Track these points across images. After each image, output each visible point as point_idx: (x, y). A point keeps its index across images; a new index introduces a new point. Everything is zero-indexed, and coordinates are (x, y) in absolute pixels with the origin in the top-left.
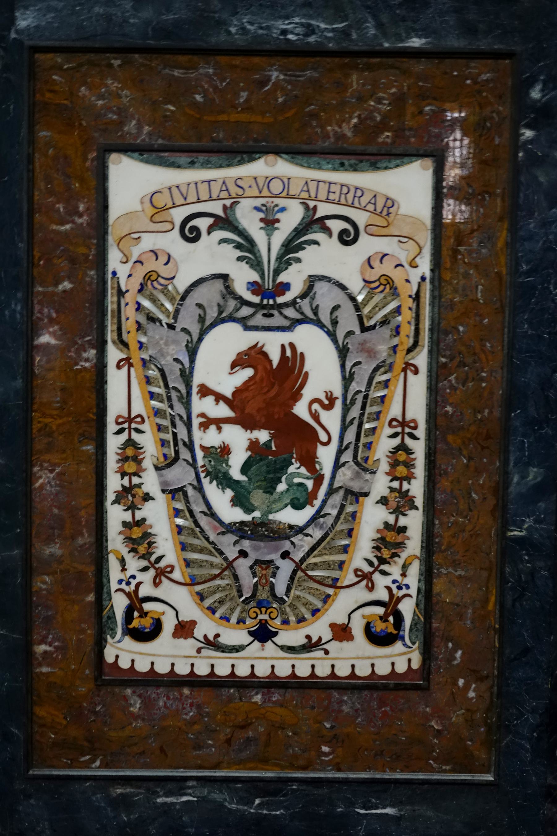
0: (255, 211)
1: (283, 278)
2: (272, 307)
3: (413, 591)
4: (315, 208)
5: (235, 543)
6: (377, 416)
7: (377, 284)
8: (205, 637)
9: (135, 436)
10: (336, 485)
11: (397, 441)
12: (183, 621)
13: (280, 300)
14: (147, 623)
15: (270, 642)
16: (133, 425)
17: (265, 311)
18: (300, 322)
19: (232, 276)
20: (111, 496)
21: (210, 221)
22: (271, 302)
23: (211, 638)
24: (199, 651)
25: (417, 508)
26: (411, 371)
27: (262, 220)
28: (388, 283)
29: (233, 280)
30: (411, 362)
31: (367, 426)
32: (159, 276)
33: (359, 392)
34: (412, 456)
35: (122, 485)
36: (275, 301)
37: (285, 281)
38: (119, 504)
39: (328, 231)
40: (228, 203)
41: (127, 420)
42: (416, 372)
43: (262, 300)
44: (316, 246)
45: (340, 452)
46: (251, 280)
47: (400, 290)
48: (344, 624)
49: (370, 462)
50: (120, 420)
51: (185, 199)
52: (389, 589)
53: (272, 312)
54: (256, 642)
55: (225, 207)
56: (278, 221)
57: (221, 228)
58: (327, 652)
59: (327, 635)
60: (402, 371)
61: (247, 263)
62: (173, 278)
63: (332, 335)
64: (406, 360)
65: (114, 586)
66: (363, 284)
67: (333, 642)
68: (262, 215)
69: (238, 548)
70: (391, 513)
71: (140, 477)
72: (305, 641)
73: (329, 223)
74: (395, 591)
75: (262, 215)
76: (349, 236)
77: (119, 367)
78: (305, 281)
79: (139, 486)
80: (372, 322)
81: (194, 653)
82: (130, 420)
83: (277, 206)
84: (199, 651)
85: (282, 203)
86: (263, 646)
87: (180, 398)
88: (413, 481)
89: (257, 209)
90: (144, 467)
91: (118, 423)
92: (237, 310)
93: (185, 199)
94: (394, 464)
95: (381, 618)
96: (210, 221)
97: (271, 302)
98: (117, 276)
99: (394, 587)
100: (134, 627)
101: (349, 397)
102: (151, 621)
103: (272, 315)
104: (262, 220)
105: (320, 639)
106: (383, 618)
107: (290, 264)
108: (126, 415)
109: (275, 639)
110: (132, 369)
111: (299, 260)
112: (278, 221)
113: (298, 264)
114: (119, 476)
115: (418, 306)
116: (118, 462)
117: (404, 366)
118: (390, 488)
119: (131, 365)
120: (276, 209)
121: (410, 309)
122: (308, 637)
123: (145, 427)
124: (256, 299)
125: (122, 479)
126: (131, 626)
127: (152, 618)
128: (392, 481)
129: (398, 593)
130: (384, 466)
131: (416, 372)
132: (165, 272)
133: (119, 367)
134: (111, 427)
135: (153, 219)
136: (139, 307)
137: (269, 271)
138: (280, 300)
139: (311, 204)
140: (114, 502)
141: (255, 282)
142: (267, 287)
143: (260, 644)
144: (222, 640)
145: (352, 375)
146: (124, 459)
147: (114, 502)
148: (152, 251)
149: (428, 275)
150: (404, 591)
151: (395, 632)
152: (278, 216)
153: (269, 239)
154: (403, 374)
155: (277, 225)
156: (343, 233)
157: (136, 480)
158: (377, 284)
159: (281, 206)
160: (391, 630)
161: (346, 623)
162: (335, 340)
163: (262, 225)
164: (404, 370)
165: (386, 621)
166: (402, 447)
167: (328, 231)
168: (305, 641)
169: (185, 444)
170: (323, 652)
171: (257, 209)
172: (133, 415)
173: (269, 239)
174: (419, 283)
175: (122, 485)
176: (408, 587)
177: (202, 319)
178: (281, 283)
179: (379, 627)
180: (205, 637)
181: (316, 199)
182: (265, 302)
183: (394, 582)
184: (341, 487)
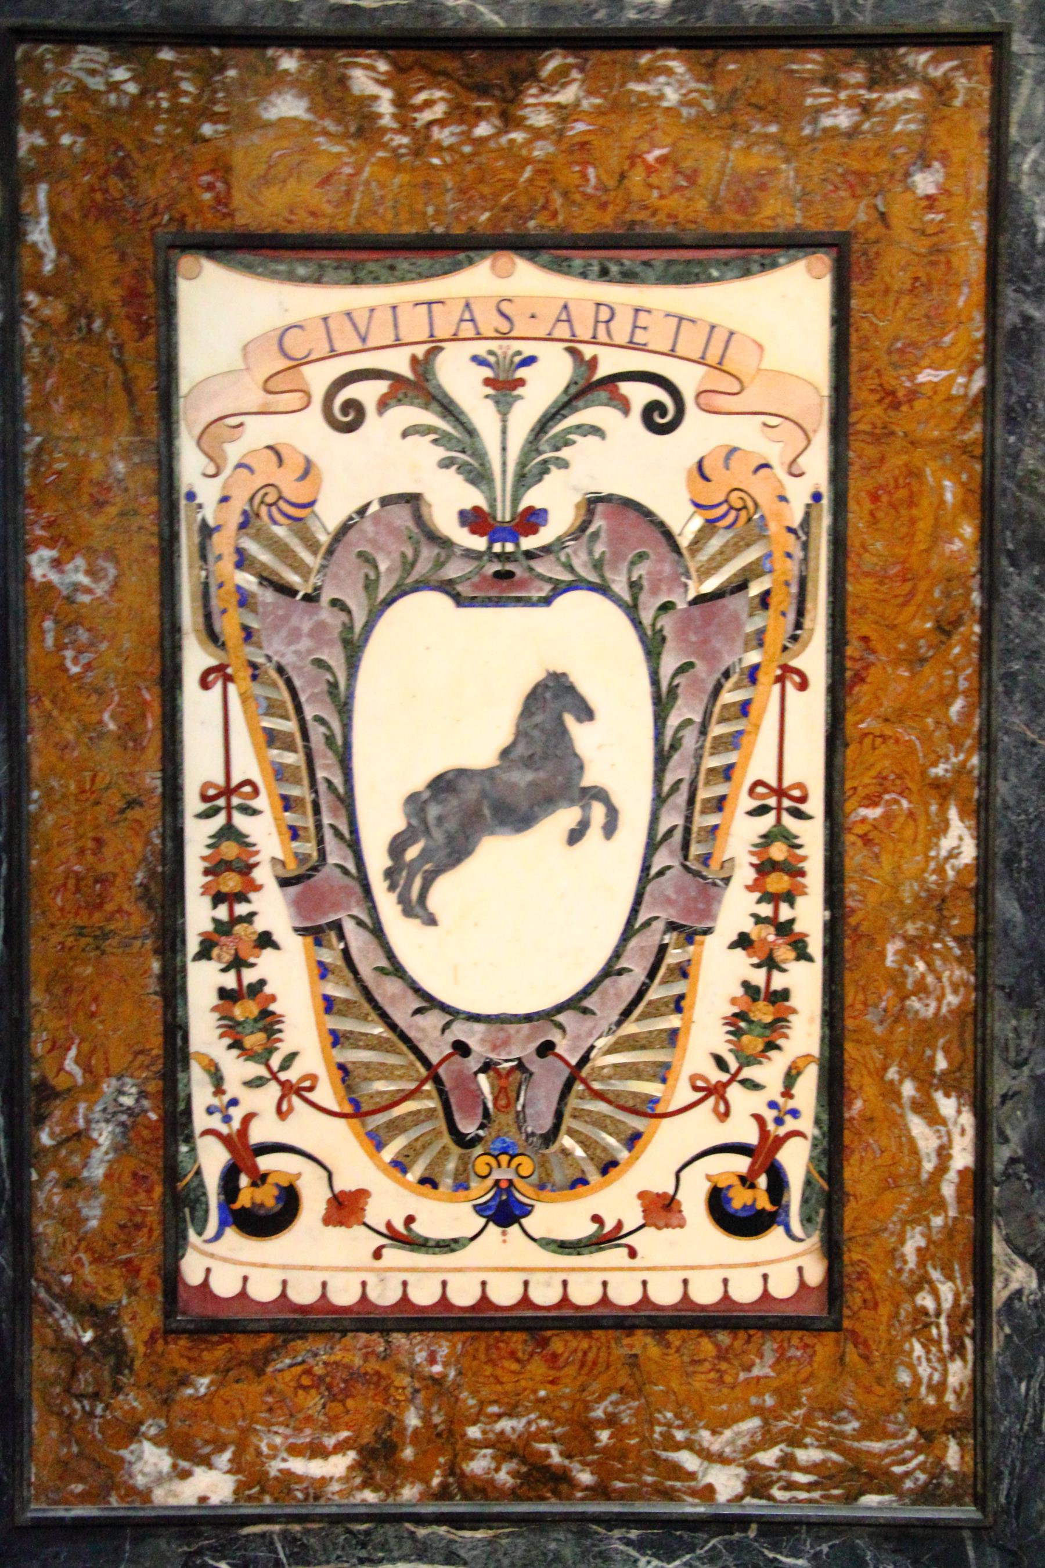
0: (474, 365)
1: (533, 498)
3: (806, 1124)
6: (727, 773)
7: (724, 508)
9: (240, 821)
11: (768, 821)
12: (342, 1192)
13: (528, 543)
14: (267, 1197)
16: (236, 801)
18: (570, 587)
19: (429, 497)
20: (193, 946)
22: (510, 547)
23: (399, 1226)
24: (377, 1254)
25: (809, 959)
26: (794, 683)
27: (487, 382)
28: (745, 507)
29: (429, 506)
30: (794, 663)
31: (703, 794)
32: (280, 498)
33: (689, 722)
34: (799, 852)
35: (215, 921)
37: (538, 505)
38: (210, 958)
40: (420, 351)
45: (652, 846)
46: (468, 506)
48: (665, 1194)
49: (714, 864)
50: (211, 792)
51: (364, 340)
52: (759, 1119)
56: (521, 382)
58: (633, 1253)
59: (633, 1217)
62: (312, 504)
63: (632, 610)
66: (692, 508)
67: (649, 1231)
68: (488, 373)
72: (593, 1228)
73: (626, 388)
75: (488, 373)
76: (663, 414)
77: (205, 684)
78: (578, 506)
82: (228, 791)
83: (519, 353)
84: (377, 1254)
85: (528, 349)
88: (800, 901)
89: (477, 360)
90: (259, 882)
91: (205, 798)
92: (439, 564)
93: (364, 340)
94: (765, 868)
97: (510, 547)
98: (198, 501)
99: (769, 1115)
101: (669, 733)
104: (487, 382)
105: (620, 1225)
106: (747, 1181)
107: (547, 471)
108: (220, 780)
110: (232, 688)
112: (521, 382)
113: (563, 471)
114: (207, 901)
116: (207, 872)
117: (779, 672)
118: (754, 915)
119: (228, 679)
120: (517, 359)
123: (261, 802)
124: (480, 543)
125: (215, 906)
126: (237, 1206)
128: (759, 901)
130: (744, 874)
132: (295, 492)
133: (205, 684)
134: (192, 803)
136: (243, 561)
137: (503, 483)
138: (528, 543)
139: (588, 351)
141: (477, 509)
142: (499, 518)
145: (673, 691)
146: (215, 868)
148: (270, 447)
149: (824, 488)
150: (791, 1124)
151: (769, 1207)
152: (521, 373)
153: (504, 421)
154: (777, 687)
155: (520, 391)
156: (652, 409)
158: (724, 508)
159: (527, 353)
160: (764, 1203)
161: (671, 1192)
162: (637, 623)
163: (489, 391)
164: (780, 680)
165: (753, 1186)
166: (778, 834)
168: (593, 1228)
170: (625, 1251)
171: (477, 360)
172: (235, 781)
173: (504, 421)
174: (808, 506)
175: (215, 921)
177: (370, 586)
178: (531, 511)
179: (740, 1199)
180: (389, 1225)
181: (594, 341)
182: (497, 548)
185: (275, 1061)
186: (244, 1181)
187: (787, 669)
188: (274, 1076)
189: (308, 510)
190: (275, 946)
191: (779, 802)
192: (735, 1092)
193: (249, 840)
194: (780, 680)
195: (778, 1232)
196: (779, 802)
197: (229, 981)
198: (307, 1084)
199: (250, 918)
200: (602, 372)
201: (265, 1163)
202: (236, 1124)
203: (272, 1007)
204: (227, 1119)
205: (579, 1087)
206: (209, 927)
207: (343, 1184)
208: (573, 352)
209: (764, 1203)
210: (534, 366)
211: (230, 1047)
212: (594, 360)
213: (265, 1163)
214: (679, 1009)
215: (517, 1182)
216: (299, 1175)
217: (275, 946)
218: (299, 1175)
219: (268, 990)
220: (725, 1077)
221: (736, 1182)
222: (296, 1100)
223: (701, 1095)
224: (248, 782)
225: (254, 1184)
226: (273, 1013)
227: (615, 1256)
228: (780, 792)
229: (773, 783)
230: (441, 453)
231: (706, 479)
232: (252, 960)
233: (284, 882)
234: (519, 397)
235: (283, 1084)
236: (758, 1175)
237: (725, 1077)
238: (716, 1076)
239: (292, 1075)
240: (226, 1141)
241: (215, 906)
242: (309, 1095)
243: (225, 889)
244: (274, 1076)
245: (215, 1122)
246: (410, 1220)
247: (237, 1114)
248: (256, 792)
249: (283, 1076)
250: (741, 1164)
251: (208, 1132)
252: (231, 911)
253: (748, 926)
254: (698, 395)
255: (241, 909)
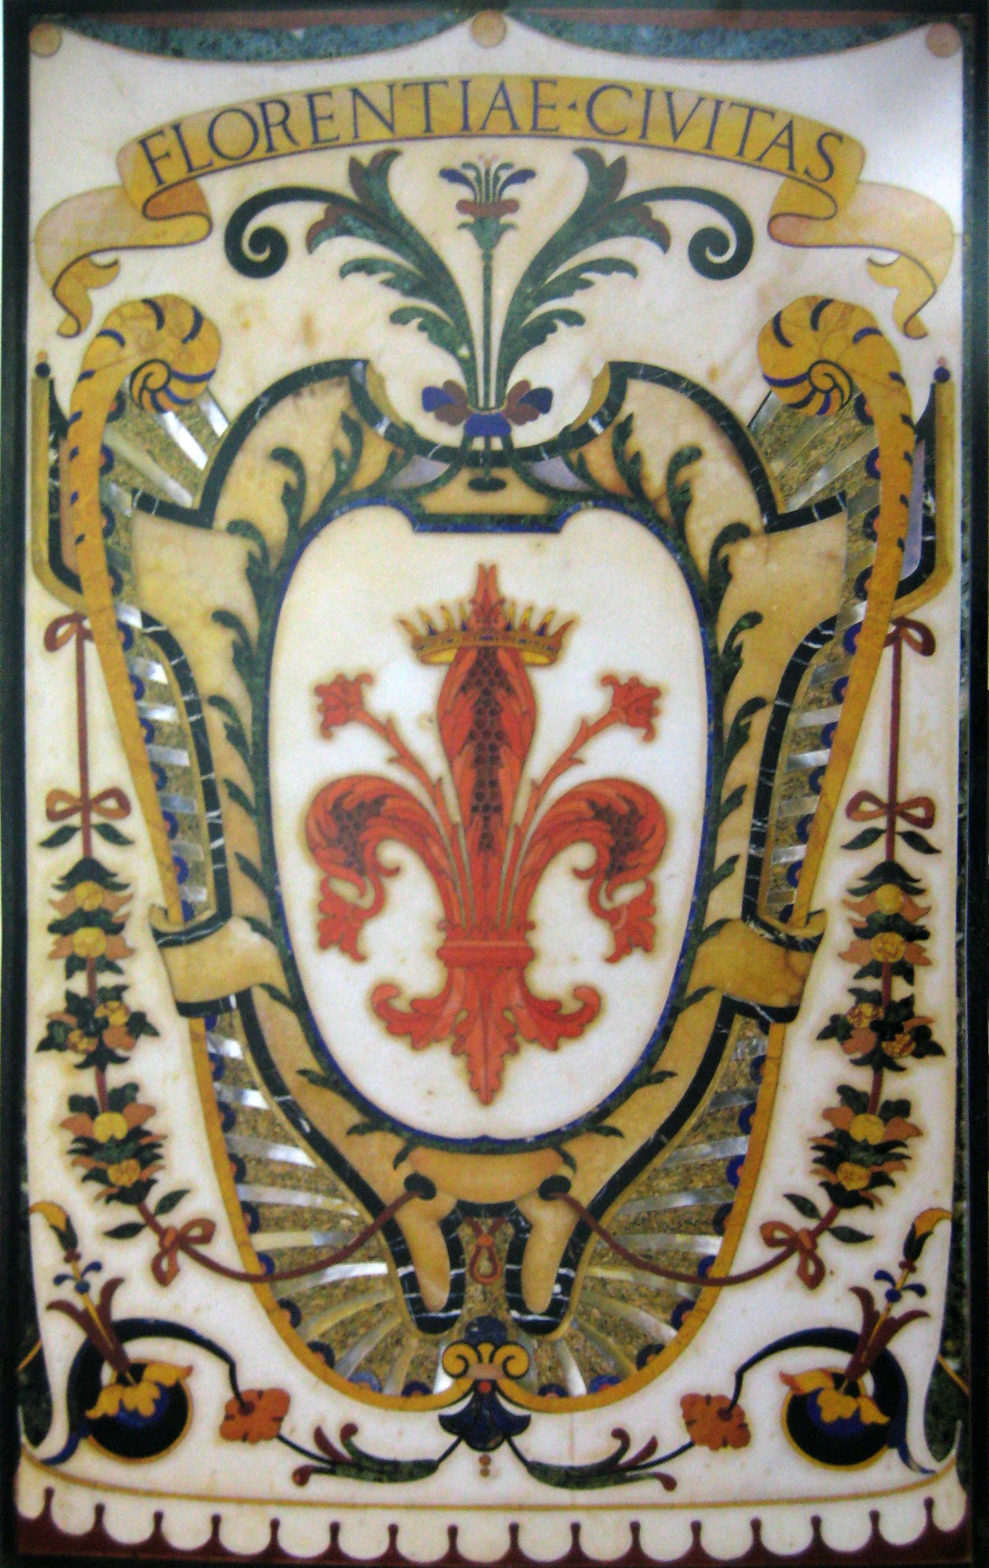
0: (444, 183)
2: (499, 459)
3: (935, 1302)
4: (621, 164)
5: (400, 1158)
8: (319, 1436)
10: (695, 983)
15: (505, 1447)
17: (479, 472)
20: (36, 1031)
21: (314, 211)
25: (937, 1050)
30: (917, 616)
36: (508, 442)
37: (536, 383)
39: (662, 237)
40: (365, 155)
41: (80, 804)
42: (928, 646)
43: (467, 439)
44: (625, 276)
47: (874, 407)
48: (721, 1398)
52: (864, 1296)
53: (498, 473)
54: (463, 1446)
55: (356, 171)
56: (513, 206)
57: (347, 231)
60: (886, 644)
61: (422, 328)
64: (896, 613)
65: (44, 1291)
68: (464, 193)
69: (406, 1169)
70: (856, 1063)
71: (119, 971)
73: (663, 211)
74: (880, 1303)
76: (722, 250)
79: (118, 992)
80: (797, 502)
81: (288, 1488)
82: (85, 804)
84: (301, 1476)
86: (485, 1462)
87: (235, 736)
91: (52, 815)
95: (837, 1379)
96: (314, 211)
97: (497, 444)
99: (879, 1291)
100: (105, 1419)
102: (155, 1393)
103: (498, 485)
104: (463, 206)
109: (518, 1440)
111: (574, 319)
112: (513, 206)
115: (931, 450)
117: (892, 629)
118: (853, 991)
121: (907, 457)
122: (620, 1434)
123: (133, 825)
124: (450, 436)
126: (94, 1413)
127: (159, 1385)
129: (888, 1310)
131: (928, 646)
135: (150, 211)
139: (610, 154)
140: (45, 1045)
142: (481, 403)
143: (477, 1455)
144: (368, 1443)
147: (45, 1045)
150: (909, 1301)
152: (511, 192)
153: (487, 259)
154: (889, 652)
157: (107, 980)
161: (730, 1394)
163: (468, 219)
164: (894, 640)
165: (854, 1391)
167: (662, 237)
169: (246, 867)
173: (487, 259)
176: (920, 1291)
180: (319, 1436)
183: (882, 1275)
184: (705, 991)
185: (152, 1200)
186: (107, 1374)
187: (903, 623)
188: (150, 1221)
189: (200, 387)
190: (154, 1033)
191: (892, 823)
192: (828, 1247)
193: (119, 880)
194: (894, 640)
195: (890, 1457)
196: (892, 823)
197: (86, 1084)
198: (196, 1232)
199: (118, 992)
200: (631, 188)
201: (137, 1349)
202: (95, 1294)
203: (151, 1125)
204: (83, 1288)
205: (595, 1243)
206: (60, 1004)
207: (250, 1379)
208: (590, 158)
209: (872, 1415)
210: (530, 183)
211: (86, 1178)
212: (621, 164)
213: (137, 1349)
214: (746, 1128)
215: (506, 1385)
216: (189, 1370)
217: (154, 1033)
218: (189, 1370)
219: (141, 1098)
220: (812, 1224)
221: (830, 1384)
222: (182, 1259)
223: (778, 1251)
224: (115, 793)
225: (121, 1381)
226: (147, 1134)
227: (649, 1490)
228: (893, 808)
229: (883, 795)
230: (395, 300)
231: (785, 343)
232: (121, 1052)
233: (165, 941)
234: (510, 226)
235: (161, 1233)
236: (861, 1373)
237: (812, 1224)
238: (798, 1222)
239: (175, 1219)
240: (81, 1318)
241: (70, 973)
242: (202, 1249)
243: (81, 952)
244: (150, 1221)
245: (67, 1292)
246: (349, 1431)
247: (97, 1282)
248: (125, 807)
249: (164, 1220)
250: (839, 1360)
251: (58, 1306)
252: (91, 981)
253: (845, 1004)
254: (773, 219)
255: (107, 980)
